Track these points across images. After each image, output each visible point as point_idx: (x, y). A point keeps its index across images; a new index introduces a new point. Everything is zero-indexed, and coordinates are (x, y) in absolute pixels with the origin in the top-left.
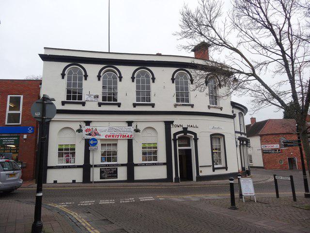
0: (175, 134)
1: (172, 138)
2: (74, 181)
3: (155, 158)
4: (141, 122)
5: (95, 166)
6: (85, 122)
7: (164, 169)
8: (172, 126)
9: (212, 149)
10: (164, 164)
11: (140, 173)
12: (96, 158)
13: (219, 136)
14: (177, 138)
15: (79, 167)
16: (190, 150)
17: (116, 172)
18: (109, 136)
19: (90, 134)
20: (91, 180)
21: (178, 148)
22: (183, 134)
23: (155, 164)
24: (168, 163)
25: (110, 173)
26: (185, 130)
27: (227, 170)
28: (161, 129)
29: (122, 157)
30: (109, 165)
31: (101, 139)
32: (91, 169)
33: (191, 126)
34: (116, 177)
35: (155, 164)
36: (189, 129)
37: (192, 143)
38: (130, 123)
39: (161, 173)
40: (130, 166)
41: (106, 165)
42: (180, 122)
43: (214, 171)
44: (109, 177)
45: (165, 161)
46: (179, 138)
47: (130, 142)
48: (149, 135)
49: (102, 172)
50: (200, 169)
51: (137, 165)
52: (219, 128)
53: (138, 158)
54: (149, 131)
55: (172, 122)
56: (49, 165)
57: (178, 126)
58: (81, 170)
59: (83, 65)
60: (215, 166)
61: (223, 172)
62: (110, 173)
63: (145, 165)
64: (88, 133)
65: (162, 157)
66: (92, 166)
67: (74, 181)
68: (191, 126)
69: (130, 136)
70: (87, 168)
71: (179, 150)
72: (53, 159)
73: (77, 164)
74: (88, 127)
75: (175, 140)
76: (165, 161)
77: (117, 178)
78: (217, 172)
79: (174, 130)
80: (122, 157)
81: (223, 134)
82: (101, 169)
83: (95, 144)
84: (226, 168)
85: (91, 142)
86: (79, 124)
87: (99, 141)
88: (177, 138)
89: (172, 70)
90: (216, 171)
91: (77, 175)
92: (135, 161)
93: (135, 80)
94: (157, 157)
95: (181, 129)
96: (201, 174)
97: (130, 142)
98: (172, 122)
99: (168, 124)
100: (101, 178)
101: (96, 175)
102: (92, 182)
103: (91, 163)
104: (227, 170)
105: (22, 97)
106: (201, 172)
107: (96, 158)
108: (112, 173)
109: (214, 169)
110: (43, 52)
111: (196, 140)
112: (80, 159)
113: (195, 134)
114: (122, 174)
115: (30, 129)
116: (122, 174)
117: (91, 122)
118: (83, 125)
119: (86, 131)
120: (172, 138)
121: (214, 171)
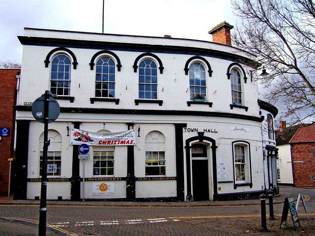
0: (188, 141)
1: (184, 145)
2: (60, 198)
4: (147, 124)
6: (73, 123)
7: (173, 184)
8: (184, 130)
11: (144, 189)
14: (190, 145)
15: (66, 180)
16: (207, 161)
18: (104, 143)
19: (79, 139)
20: (81, 198)
21: (191, 159)
22: (198, 141)
24: (179, 179)
26: (201, 136)
27: (251, 187)
28: (170, 133)
31: (94, 147)
32: (81, 183)
33: (209, 131)
36: (206, 135)
37: (210, 152)
38: (130, 125)
39: (169, 189)
42: (196, 125)
43: (235, 188)
45: (174, 175)
46: (194, 146)
47: (131, 150)
48: (155, 141)
50: (219, 185)
53: (140, 171)
54: (155, 135)
57: (192, 131)
58: (68, 185)
59: (74, 50)
60: (237, 182)
61: (247, 189)
63: (148, 179)
64: (77, 138)
66: (82, 180)
67: (60, 198)
68: (209, 131)
69: (130, 142)
73: (62, 176)
74: (76, 130)
75: (188, 147)
78: (240, 190)
79: (186, 135)
83: (86, 152)
84: (251, 185)
86: (66, 125)
87: (91, 148)
88: (190, 145)
89: (186, 57)
92: (137, 175)
95: (195, 134)
96: (219, 192)
97: (131, 150)
98: (185, 125)
99: (179, 129)
102: (81, 200)
103: (81, 175)
104: (251, 187)
106: (220, 189)
107: (87, 169)
109: (236, 186)
110: (25, 34)
111: (214, 148)
112: (67, 171)
113: (213, 141)
115: (5, 131)
117: (81, 123)
118: (72, 126)
119: (75, 135)
120: (184, 145)
121: (235, 188)
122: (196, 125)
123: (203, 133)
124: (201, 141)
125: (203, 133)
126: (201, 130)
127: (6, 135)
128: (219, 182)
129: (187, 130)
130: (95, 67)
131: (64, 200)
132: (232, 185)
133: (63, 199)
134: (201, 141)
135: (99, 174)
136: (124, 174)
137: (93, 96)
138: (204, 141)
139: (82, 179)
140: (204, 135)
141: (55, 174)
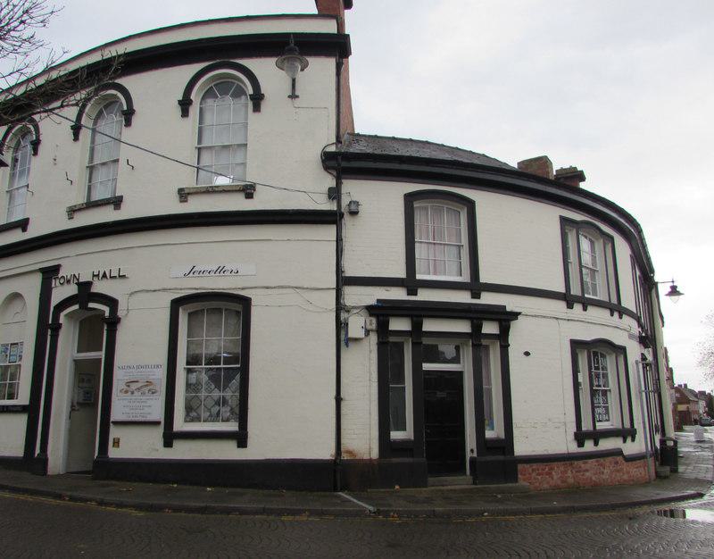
33: (104, 275)
36: (99, 287)
43: (168, 443)
50: (114, 432)
52: (221, 270)
55: (56, 269)
61: (226, 452)
68: (104, 275)
78: (184, 451)
84: (241, 439)
90: (178, 444)
95: (72, 290)
96: (113, 453)
98: (56, 269)
106: (117, 443)
109: (170, 438)
113: (112, 303)
121: (168, 443)
123: (89, 284)
124: (84, 307)
125: (89, 284)
128: (116, 423)
129: (58, 281)
132: (160, 430)
138: (91, 305)
140: (92, 290)
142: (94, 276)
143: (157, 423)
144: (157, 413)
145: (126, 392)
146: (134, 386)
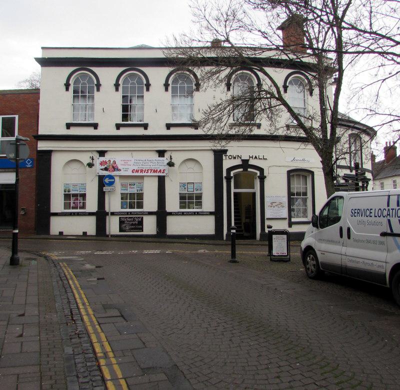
0: (229, 170)
1: (225, 174)
2: (85, 233)
3: (199, 204)
5: (113, 214)
6: (98, 152)
7: (211, 220)
8: (224, 157)
9: (290, 194)
10: (211, 213)
11: (175, 226)
12: (114, 203)
13: (304, 173)
15: (90, 214)
16: (254, 194)
17: (141, 223)
19: (106, 169)
20: (107, 233)
21: (233, 190)
22: (241, 170)
23: (198, 212)
24: (217, 214)
25: (132, 225)
26: (245, 164)
28: (208, 161)
29: (150, 203)
30: (131, 213)
31: (121, 177)
32: (107, 217)
33: (256, 157)
34: (142, 230)
35: (198, 214)
36: (252, 162)
37: (257, 183)
38: (161, 153)
40: (162, 215)
41: (128, 213)
42: (238, 151)
44: (131, 230)
45: (212, 209)
46: (236, 175)
47: (161, 181)
48: (191, 170)
49: (121, 222)
51: (171, 214)
52: (304, 160)
53: (172, 204)
54: (191, 165)
55: (225, 151)
56: (53, 210)
57: (235, 158)
58: (93, 219)
59: (96, 70)
60: (293, 220)
62: (132, 225)
63: (183, 214)
64: (103, 167)
65: (209, 204)
66: (107, 214)
68: (256, 157)
69: (162, 171)
70: (101, 216)
71: (234, 193)
72: (57, 203)
73: (88, 210)
74: (102, 159)
75: (228, 179)
76: (212, 209)
77: (143, 231)
79: (227, 164)
80: (150, 203)
81: (312, 170)
82: (120, 218)
83: (111, 184)
85: (107, 180)
86: (90, 155)
87: (117, 179)
88: (232, 175)
90: (293, 226)
91: (88, 225)
92: (169, 209)
93: (170, 88)
94: (201, 202)
95: (238, 162)
97: (161, 181)
98: (225, 151)
99: (219, 155)
100: (121, 230)
101: (113, 226)
102: (108, 236)
103: (107, 209)
105: (17, 117)
107: (114, 203)
108: (135, 224)
109: (291, 224)
110: (40, 55)
111: (262, 178)
112: (92, 205)
113: (261, 170)
114: (150, 226)
115: (29, 162)
116: (150, 226)
117: (106, 152)
118: (96, 155)
119: (101, 164)
120: (225, 174)
121: (290, 226)
122: (238, 151)
123: (248, 161)
124: (245, 170)
125: (248, 161)
126: (245, 157)
127: (29, 166)
129: (227, 157)
130: (120, 88)
131: (89, 236)
132: (287, 222)
133: (88, 234)
134: (245, 170)
135: (126, 208)
136: (154, 207)
137: (120, 121)
138: (249, 170)
139: (108, 213)
140: (249, 163)
141: (81, 208)
142: (250, 157)
143: (286, 219)
144: (284, 213)
145: (271, 207)
146: (274, 204)
